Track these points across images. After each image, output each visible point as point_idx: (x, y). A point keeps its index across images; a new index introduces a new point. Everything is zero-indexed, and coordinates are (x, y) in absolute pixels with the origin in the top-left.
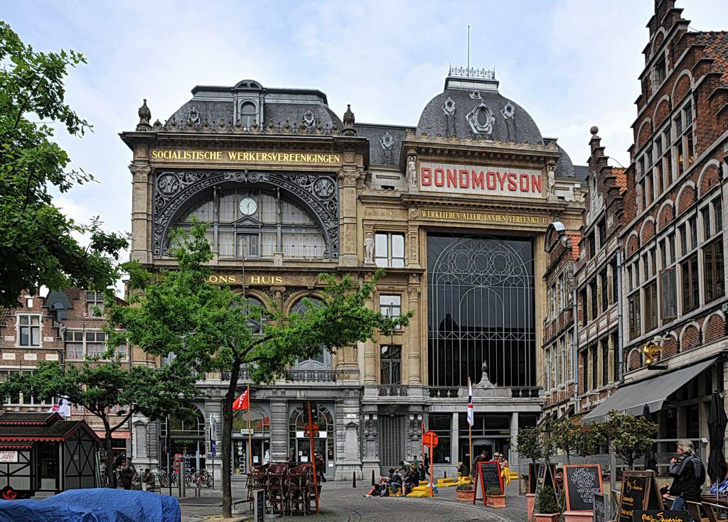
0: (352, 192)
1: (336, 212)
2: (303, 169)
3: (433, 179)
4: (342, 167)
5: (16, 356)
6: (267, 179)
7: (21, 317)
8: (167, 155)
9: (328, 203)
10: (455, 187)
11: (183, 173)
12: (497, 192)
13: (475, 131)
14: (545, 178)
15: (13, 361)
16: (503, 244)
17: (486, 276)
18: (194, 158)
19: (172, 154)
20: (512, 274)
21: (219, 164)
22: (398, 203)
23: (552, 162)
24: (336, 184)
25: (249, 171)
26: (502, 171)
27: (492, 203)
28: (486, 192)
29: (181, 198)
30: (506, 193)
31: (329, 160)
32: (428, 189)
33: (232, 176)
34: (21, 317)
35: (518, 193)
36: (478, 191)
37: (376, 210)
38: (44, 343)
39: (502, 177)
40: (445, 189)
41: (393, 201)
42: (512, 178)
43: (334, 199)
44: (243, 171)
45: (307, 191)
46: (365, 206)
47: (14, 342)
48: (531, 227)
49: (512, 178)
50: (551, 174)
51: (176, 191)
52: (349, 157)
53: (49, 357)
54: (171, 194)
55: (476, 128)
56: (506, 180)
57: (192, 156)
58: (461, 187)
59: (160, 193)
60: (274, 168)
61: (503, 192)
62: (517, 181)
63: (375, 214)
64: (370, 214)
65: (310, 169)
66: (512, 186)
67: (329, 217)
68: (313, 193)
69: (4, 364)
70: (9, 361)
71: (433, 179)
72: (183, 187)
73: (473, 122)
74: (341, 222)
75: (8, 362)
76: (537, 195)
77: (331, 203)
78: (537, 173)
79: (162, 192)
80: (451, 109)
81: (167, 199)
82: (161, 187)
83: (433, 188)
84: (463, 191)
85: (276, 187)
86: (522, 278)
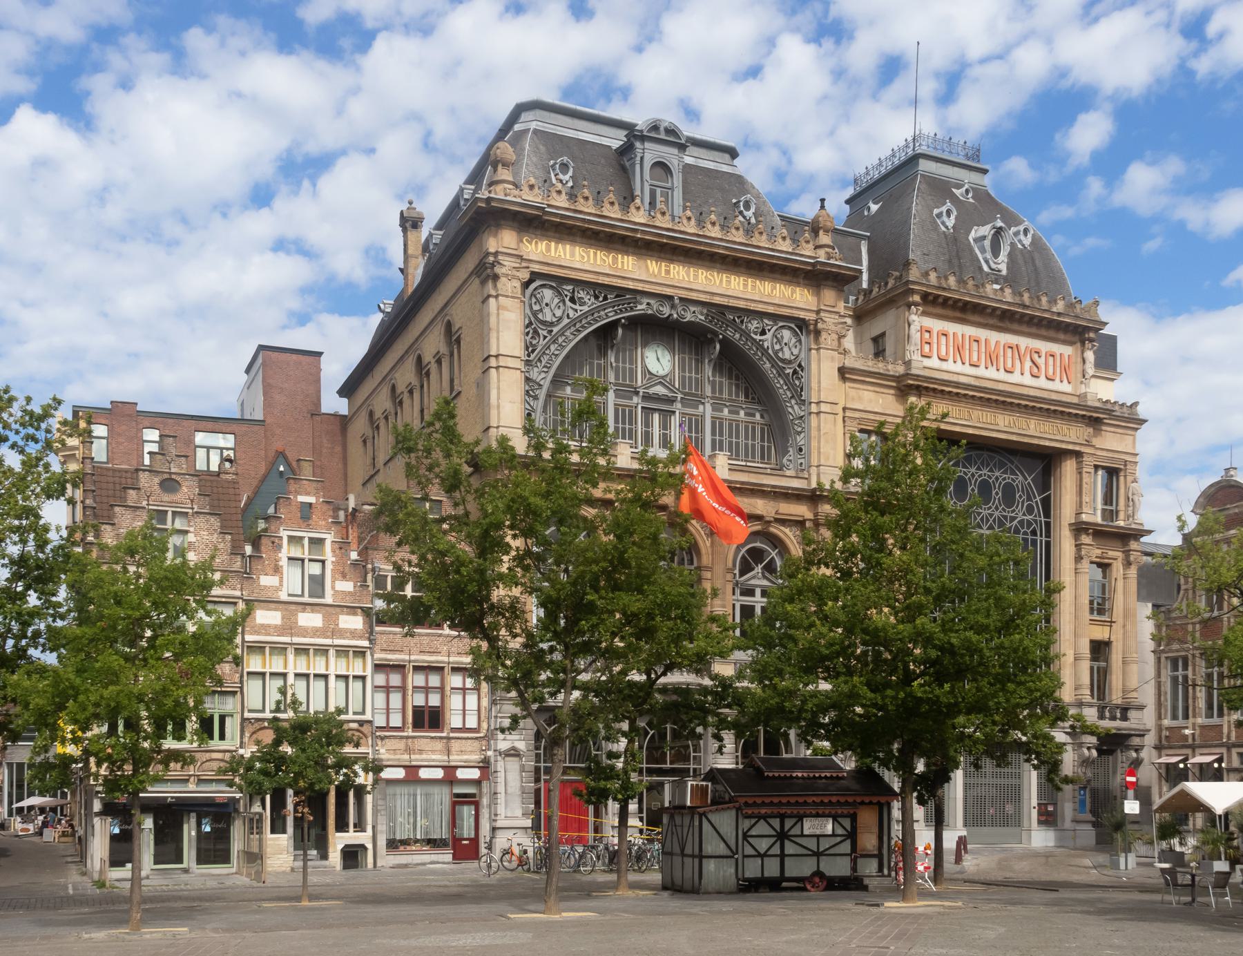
0: (833, 359)
1: (802, 390)
2: (760, 307)
3: (935, 346)
4: (818, 312)
5: (283, 618)
6: (703, 318)
7: (291, 538)
8: (548, 249)
9: (791, 371)
10: (963, 363)
11: (570, 287)
12: (1015, 378)
13: (986, 268)
14: (1079, 360)
15: (276, 626)
16: (1012, 463)
17: (991, 515)
18: (592, 261)
19: (556, 249)
20: (1024, 514)
21: (633, 279)
22: (894, 384)
23: (1092, 335)
24: (803, 338)
25: (681, 299)
26: (1024, 342)
27: (1020, 399)
28: (1002, 375)
29: (568, 333)
30: (1027, 380)
31: (798, 298)
32: (927, 362)
33: (648, 304)
34: (291, 538)
35: (1042, 382)
36: (991, 373)
37: (861, 392)
38: (336, 593)
39: (1022, 351)
40: (949, 366)
41: (889, 380)
42: (1035, 356)
43: (800, 365)
44: (670, 298)
45: (762, 346)
46: (848, 384)
47: (278, 589)
48: (1062, 442)
49: (1035, 356)
50: (1090, 356)
51: (560, 319)
52: (829, 295)
53: (346, 622)
54: (552, 324)
55: (987, 262)
56: (1028, 358)
57: (589, 257)
58: (971, 365)
59: (533, 319)
60: (717, 300)
61: (1021, 379)
62: (1041, 362)
63: (860, 399)
64: (853, 399)
65: (771, 309)
66: (1035, 370)
67: (792, 397)
68: (770, 351)
69: (258, 633)
70: (269, 626)
71: (935, 346)
72: (571, 313)
73: (983, 251)
74: (814, 408)
75: (265, 628)
76: (1066, 387)
77: (795, 372)
78: (1067, 350)
79: (536, 318)
80: (951, 222)
81: (545, 333)
82: (536, 308)
83: (934, 362)
84: (973, 371)
85: (716, 334)
86: (1036, 521)
